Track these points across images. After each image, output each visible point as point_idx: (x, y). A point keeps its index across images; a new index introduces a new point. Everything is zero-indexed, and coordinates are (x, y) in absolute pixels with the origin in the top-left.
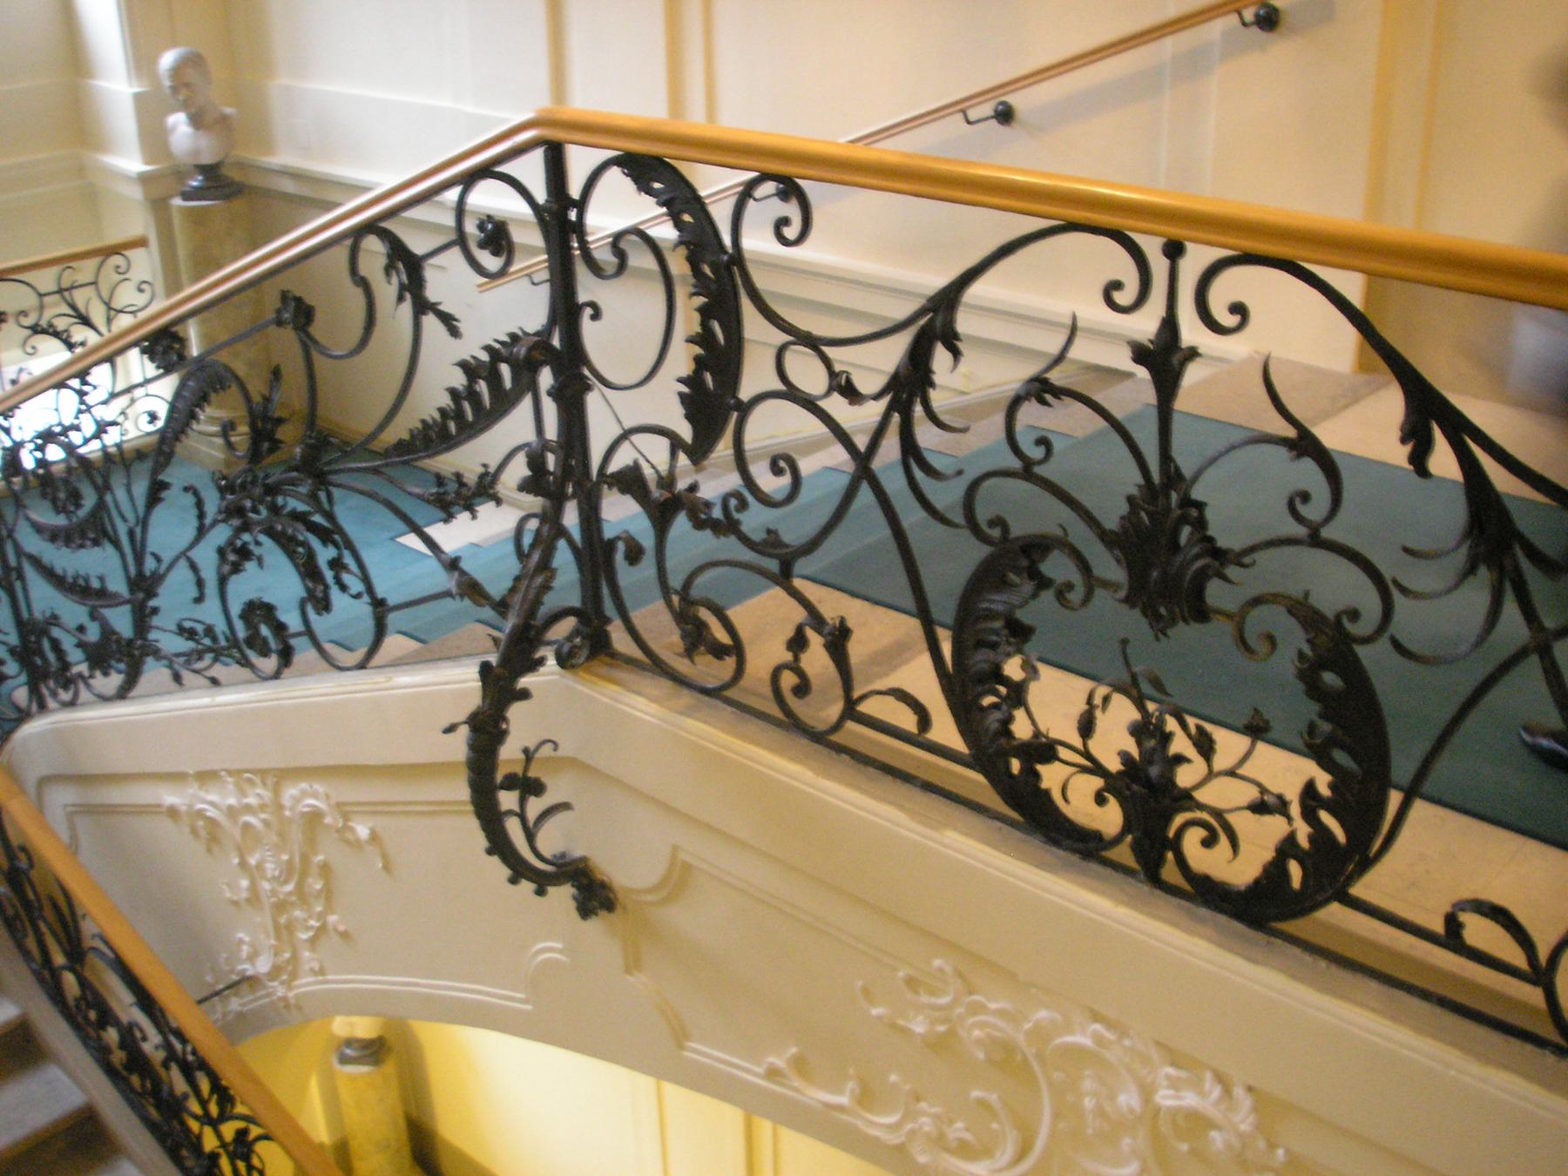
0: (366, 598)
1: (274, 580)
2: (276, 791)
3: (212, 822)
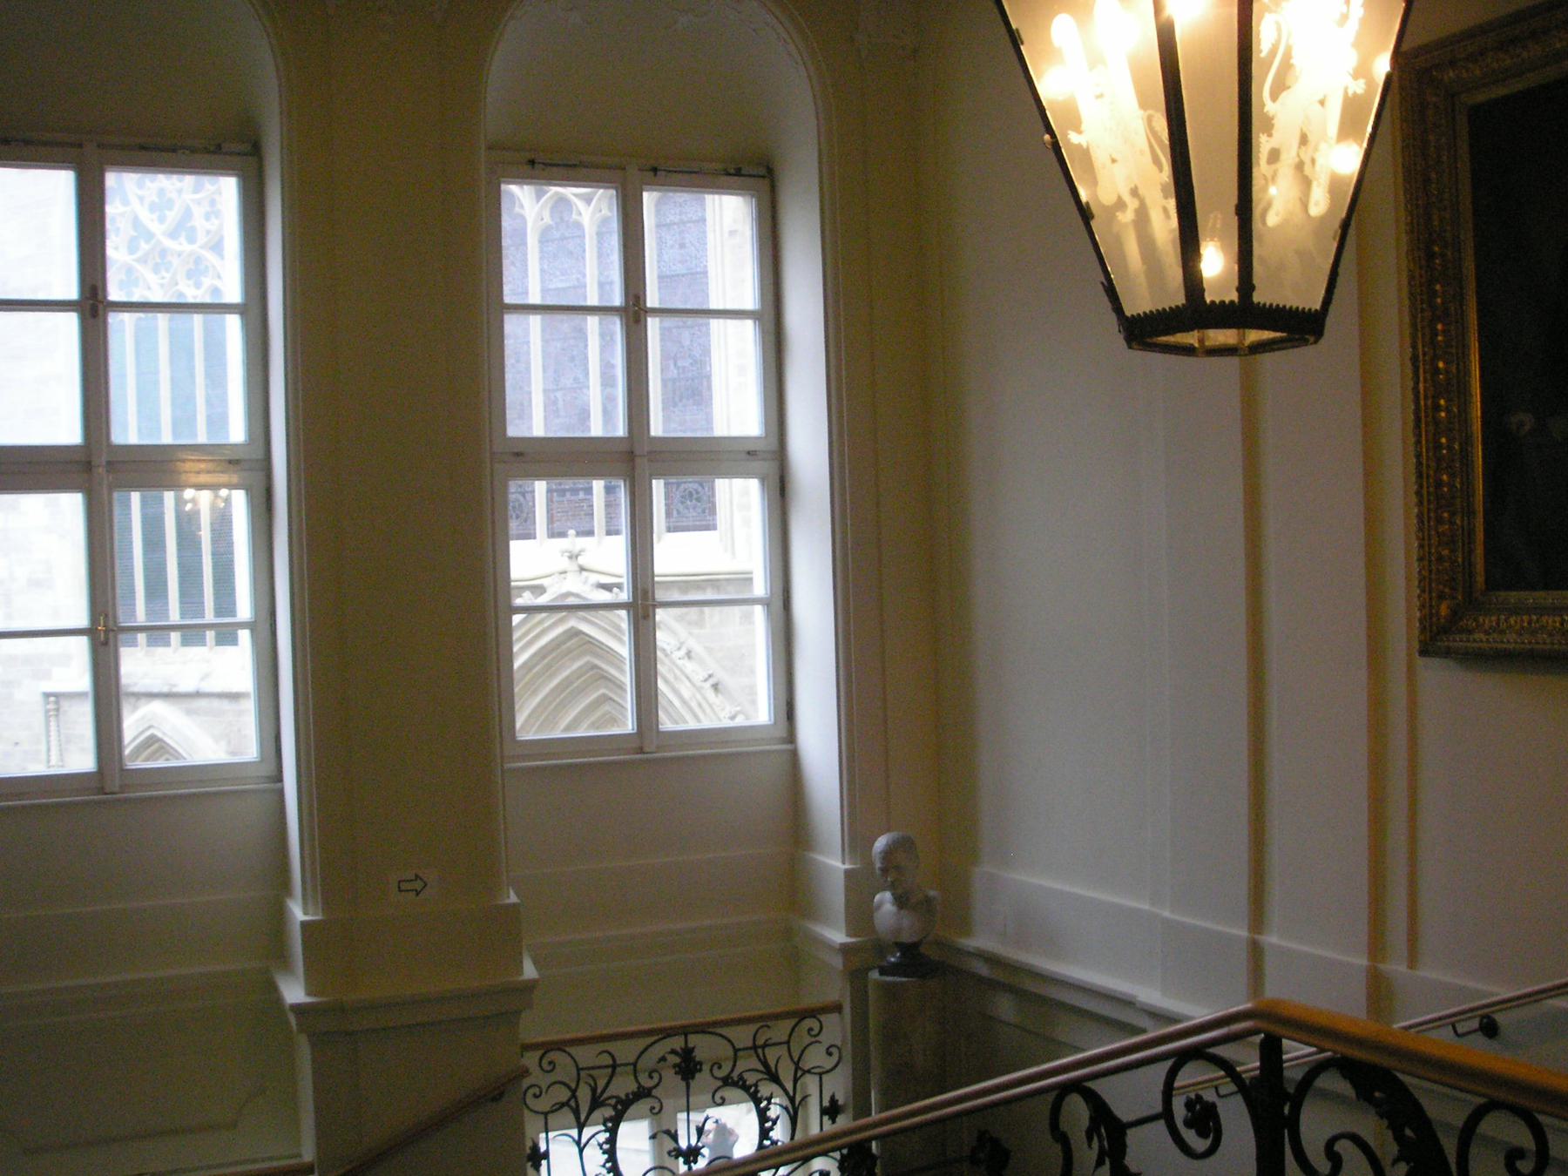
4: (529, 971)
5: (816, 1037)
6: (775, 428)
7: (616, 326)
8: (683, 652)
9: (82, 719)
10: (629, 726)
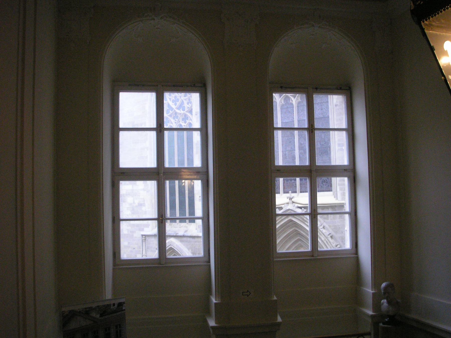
4: (279, 319)
6: (352, 163)
7: (306, 133)
8: (322, 227)
9: (154, 243)
10: (309, 249)
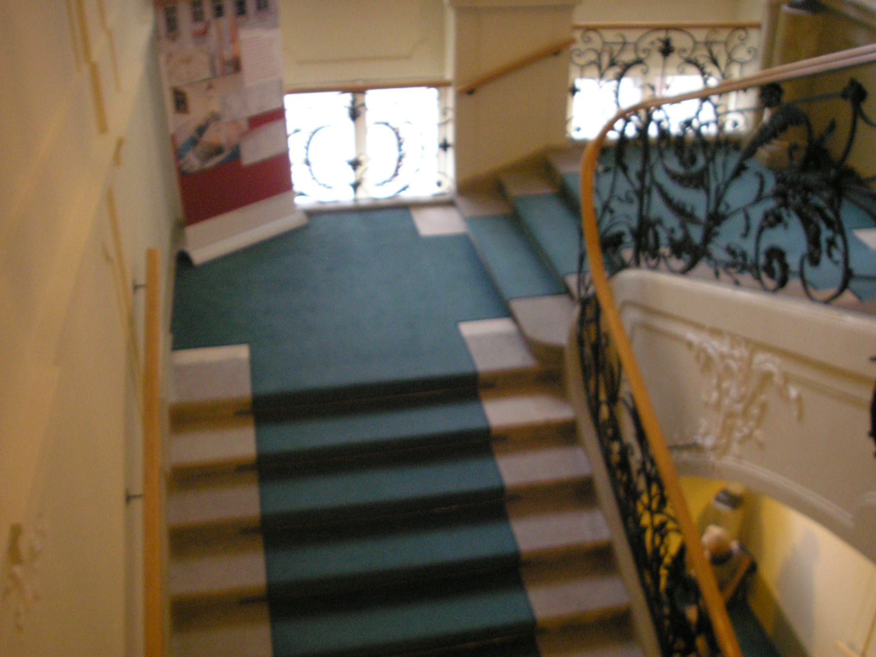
0: (841, 265)
1: (791, 238)
2: (752, 353)
3: (709, 359)
5: (743, 41)
